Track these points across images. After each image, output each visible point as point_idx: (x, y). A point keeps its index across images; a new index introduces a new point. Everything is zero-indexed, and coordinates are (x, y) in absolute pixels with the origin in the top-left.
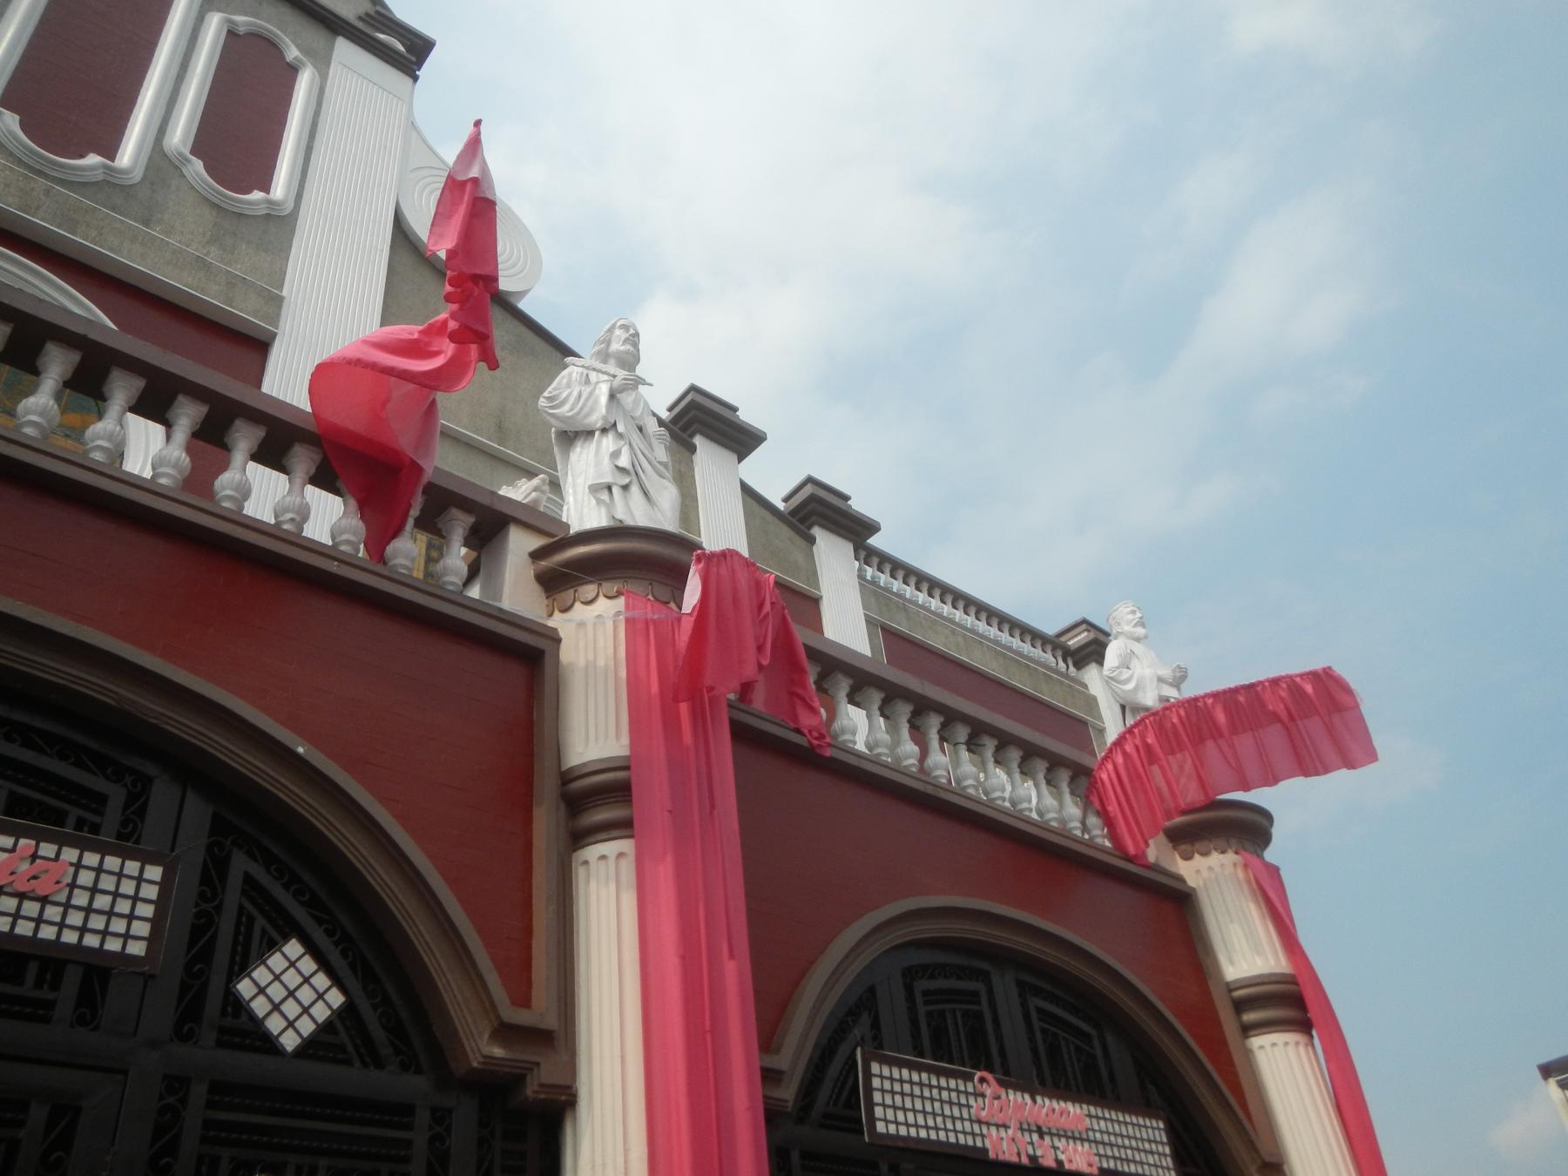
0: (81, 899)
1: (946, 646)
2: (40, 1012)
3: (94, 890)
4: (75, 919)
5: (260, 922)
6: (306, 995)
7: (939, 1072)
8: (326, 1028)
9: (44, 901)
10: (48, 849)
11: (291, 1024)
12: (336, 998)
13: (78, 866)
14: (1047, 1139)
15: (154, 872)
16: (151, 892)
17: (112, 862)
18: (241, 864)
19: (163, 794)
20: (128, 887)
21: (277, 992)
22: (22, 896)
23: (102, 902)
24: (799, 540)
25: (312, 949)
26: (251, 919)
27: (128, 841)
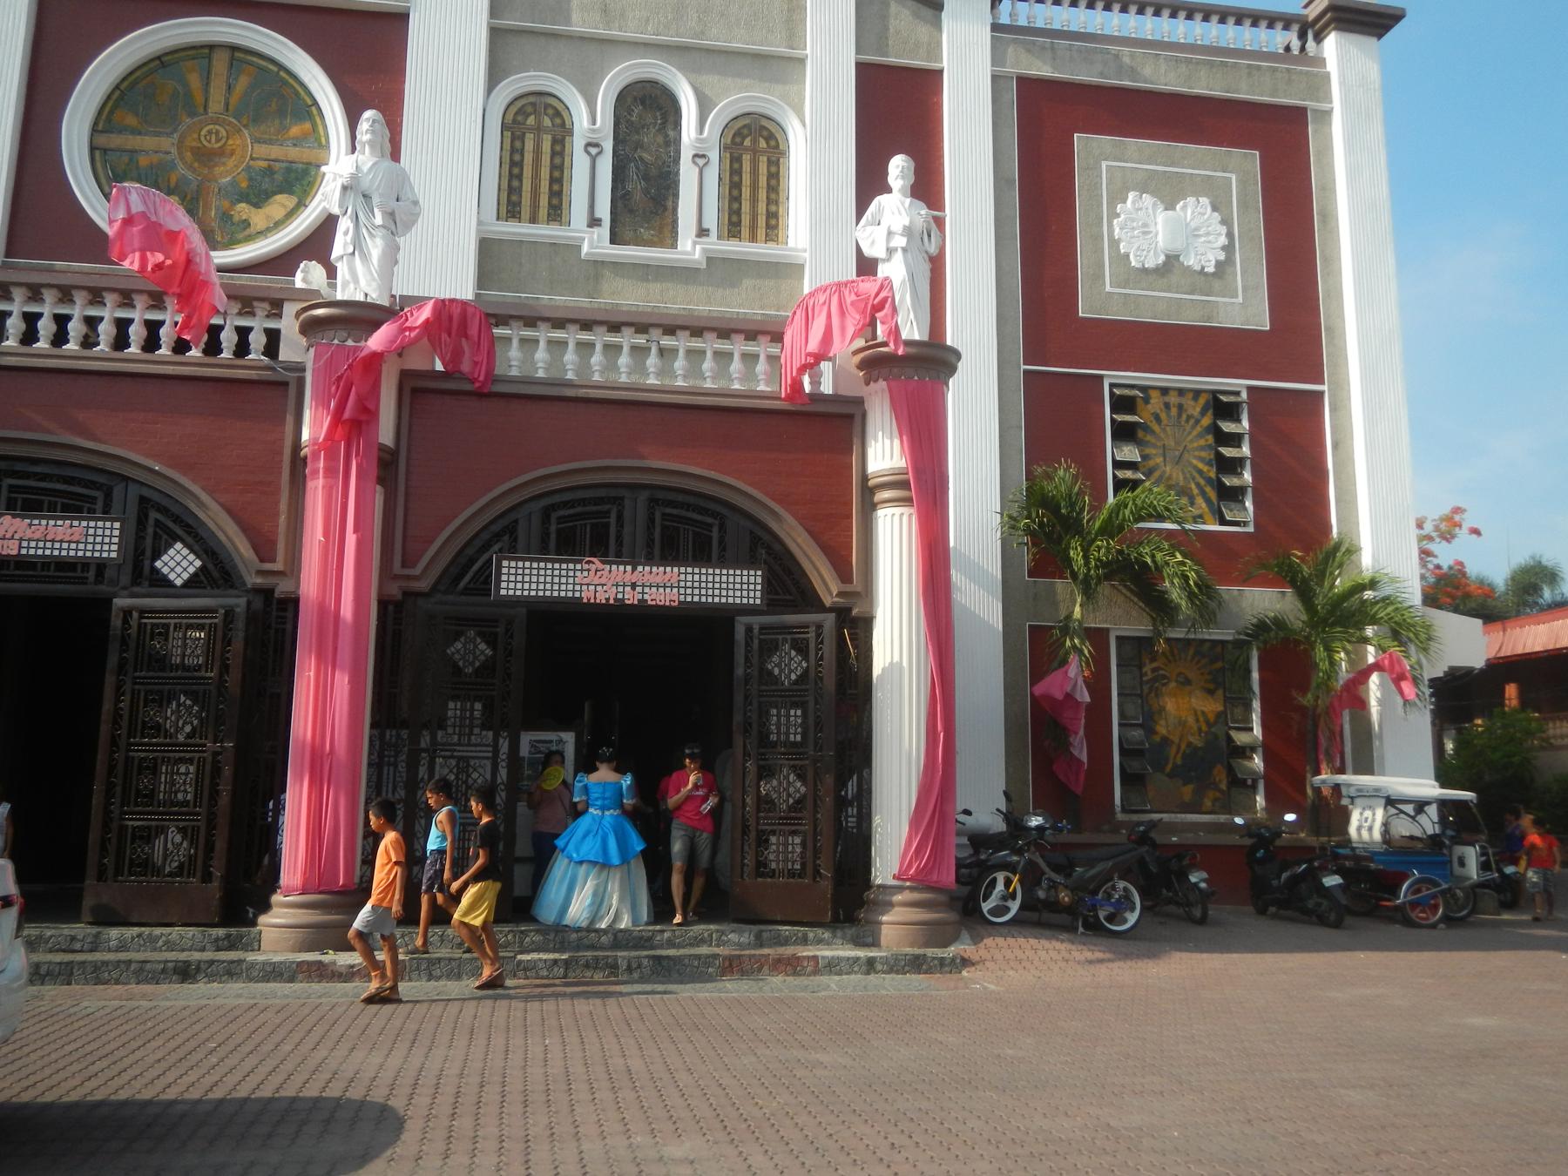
0: (91, 539)
1: (1102, 75)
2: (83, 581)
3: (95, 535)
4: (90, 547)
5: (165, 537)
6: (185, 563)
7: (553, 561)
8: (195, 575)
9: (78, 542)
10: (76, 523)
11: (179, 576)
12: (198, 563)
13: (88, 527)
14: (639, 589)
15: (117, 525)
16: (116, 533)
17: (100, 524)
18: (154, 515)
19: (118, 492)
20: (108, 532)
21: (172, 564)
22: (70, 542)
23: (99, 539)
24: (927, 12)
25: (186, 545)
26: (161, 537)
27: (107, 512)
